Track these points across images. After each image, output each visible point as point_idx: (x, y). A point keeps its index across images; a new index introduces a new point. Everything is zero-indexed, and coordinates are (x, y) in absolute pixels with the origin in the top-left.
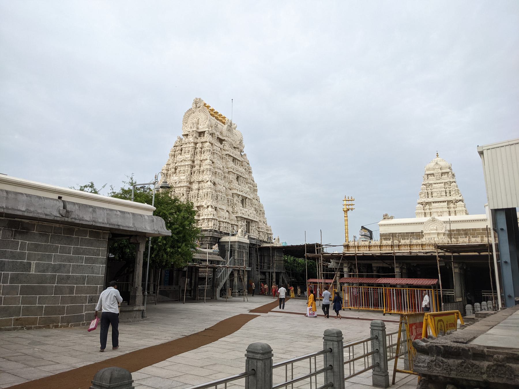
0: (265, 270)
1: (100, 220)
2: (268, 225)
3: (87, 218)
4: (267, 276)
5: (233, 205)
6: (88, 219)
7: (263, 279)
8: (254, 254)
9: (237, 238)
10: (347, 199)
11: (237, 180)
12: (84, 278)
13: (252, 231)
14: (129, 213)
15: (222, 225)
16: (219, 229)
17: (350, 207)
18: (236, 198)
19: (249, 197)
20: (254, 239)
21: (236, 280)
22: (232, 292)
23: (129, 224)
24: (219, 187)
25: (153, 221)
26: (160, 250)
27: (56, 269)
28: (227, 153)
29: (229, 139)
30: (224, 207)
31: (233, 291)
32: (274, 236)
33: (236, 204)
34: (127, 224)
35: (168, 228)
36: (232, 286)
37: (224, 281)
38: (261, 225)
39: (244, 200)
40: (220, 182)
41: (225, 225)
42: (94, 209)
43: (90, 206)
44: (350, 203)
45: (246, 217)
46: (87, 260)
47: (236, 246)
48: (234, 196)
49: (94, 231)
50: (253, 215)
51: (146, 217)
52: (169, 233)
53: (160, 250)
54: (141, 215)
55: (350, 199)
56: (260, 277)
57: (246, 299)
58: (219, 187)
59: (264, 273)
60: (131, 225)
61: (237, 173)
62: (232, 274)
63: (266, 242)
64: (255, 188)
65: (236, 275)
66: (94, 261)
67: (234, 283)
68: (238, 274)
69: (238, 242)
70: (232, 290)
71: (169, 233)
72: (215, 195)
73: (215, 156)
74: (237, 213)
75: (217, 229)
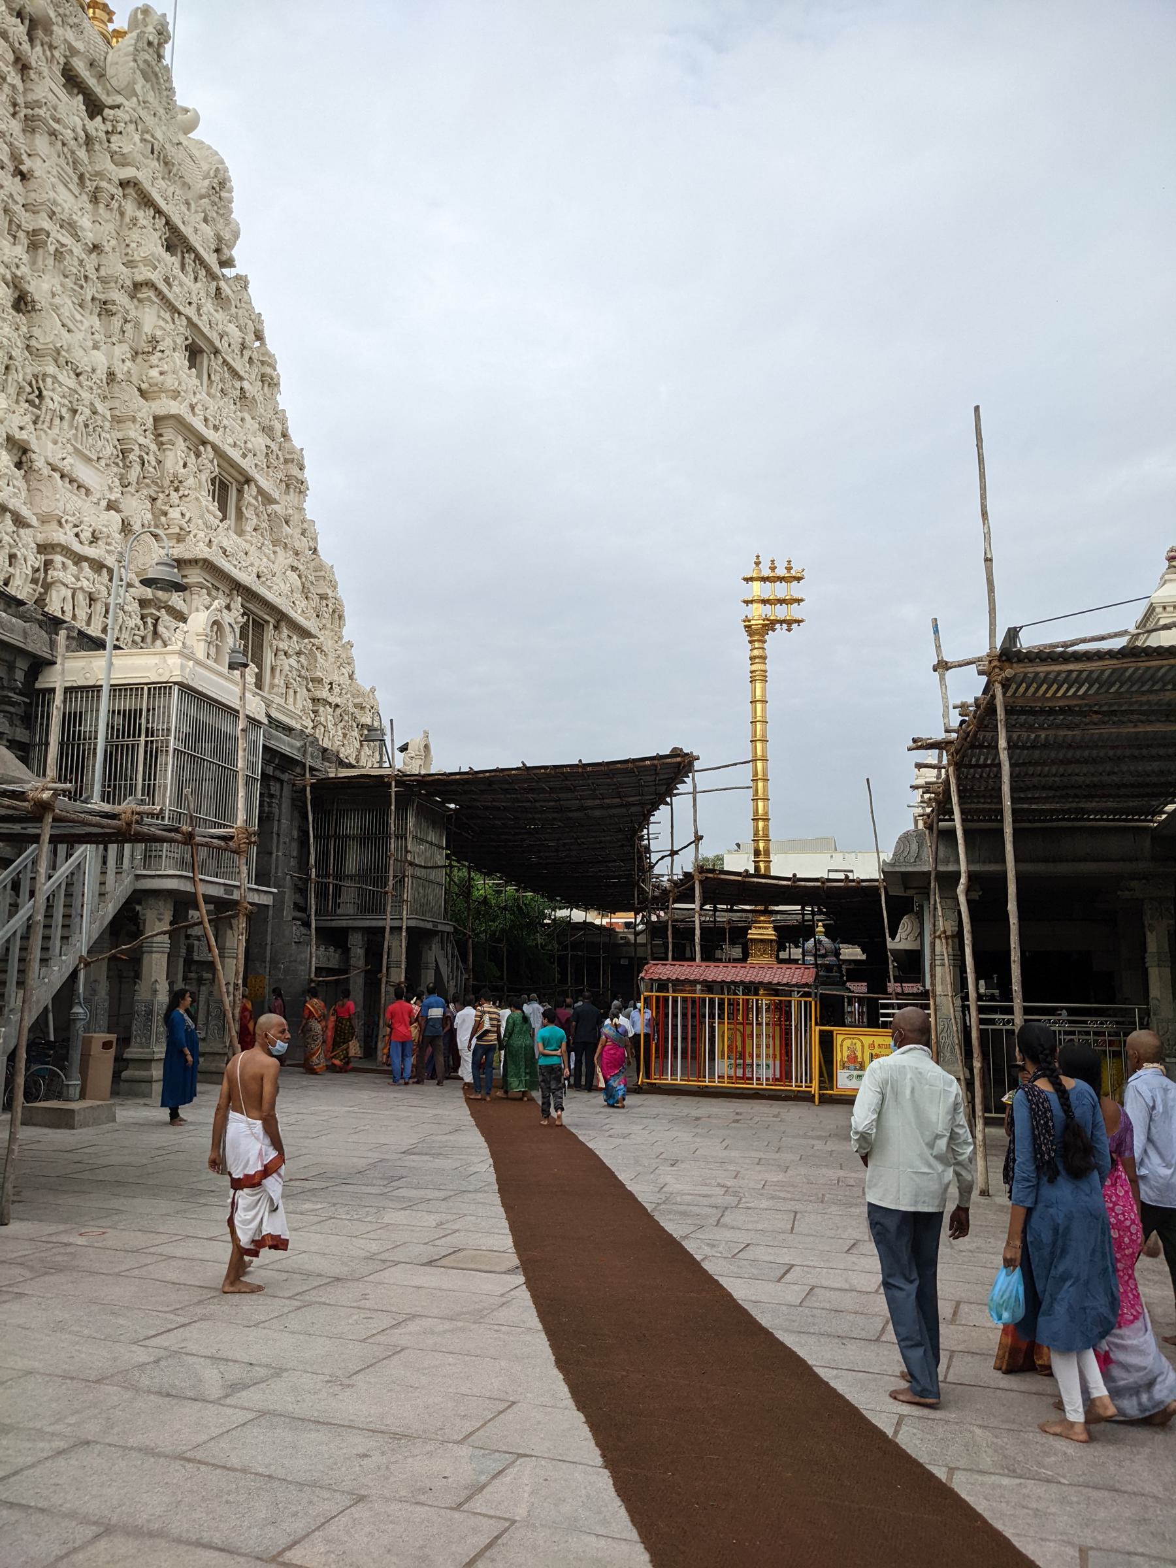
0: (347, 915)
2: (364, 680)
4: (358, 953)
5: (161, 490)
7: (330, 971)
8: (285, 823)
9: (174, 661)
10: (766, 572)
11: (192, 363)
13: (279, 680)
15: (64, 573)
16: (40, 602)
17: (781, 612)
18: (176, 455)
19: (257, 476)
20: (288, 730)
21: (157, 968)
22: (121, 1063)
24: (49, 332)
28: (128, 173)
29: (150, 121)
30: (84, 473)
31: (133, 1052)
32: (393, 742)
33: (177, 484)
36: (123, 1023)
37: (57, 974)
38: (325, 667)
39: (228, 486)
40: (67, 305)
41: (87, 579)
44: (781, 590)
45: (246, 578)
47: (173, 717)
48: (169, 434)
50: (285, 588)
55: (781, 571)
56: (314, 956)
57: (246, 1140)
58: (49, 332)
59: (334, 937)
61: (190, 312)
62: (126, 924)
63: (354, 767)
64: (295, 471)
65: (157, 924)
67: (143, 992)
68: (180, 932)
69: (187, 690)
70: (125, 1041)
72: (26, 369)
73: (41, 142)
74: (180, 539)
75: (21, 589)
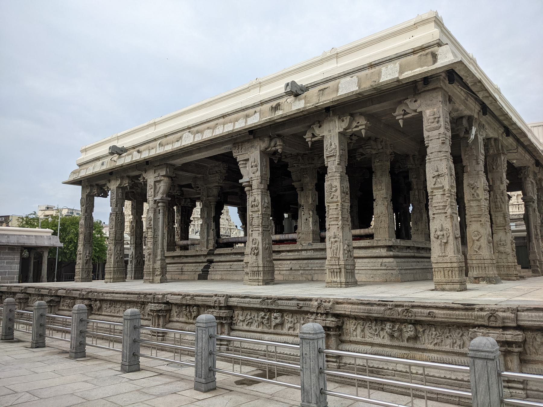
1: (13, 242)
6: (4, 242)
12: (6, 272)
14: (32, 236)
23: (32, 242)
25: (50, 239)
26: (71, 254)
34: (31, 242)
35: (61, 242)
42: (8, 236)
43: (6, 235)
46: (7, 263)
49: (12, 248)
51: (45, 237)
52: (62, 245)
53: (71, 254)
54: (41, 236)
60: (34, 242)
66: (12, 263)
71: (62, 245)
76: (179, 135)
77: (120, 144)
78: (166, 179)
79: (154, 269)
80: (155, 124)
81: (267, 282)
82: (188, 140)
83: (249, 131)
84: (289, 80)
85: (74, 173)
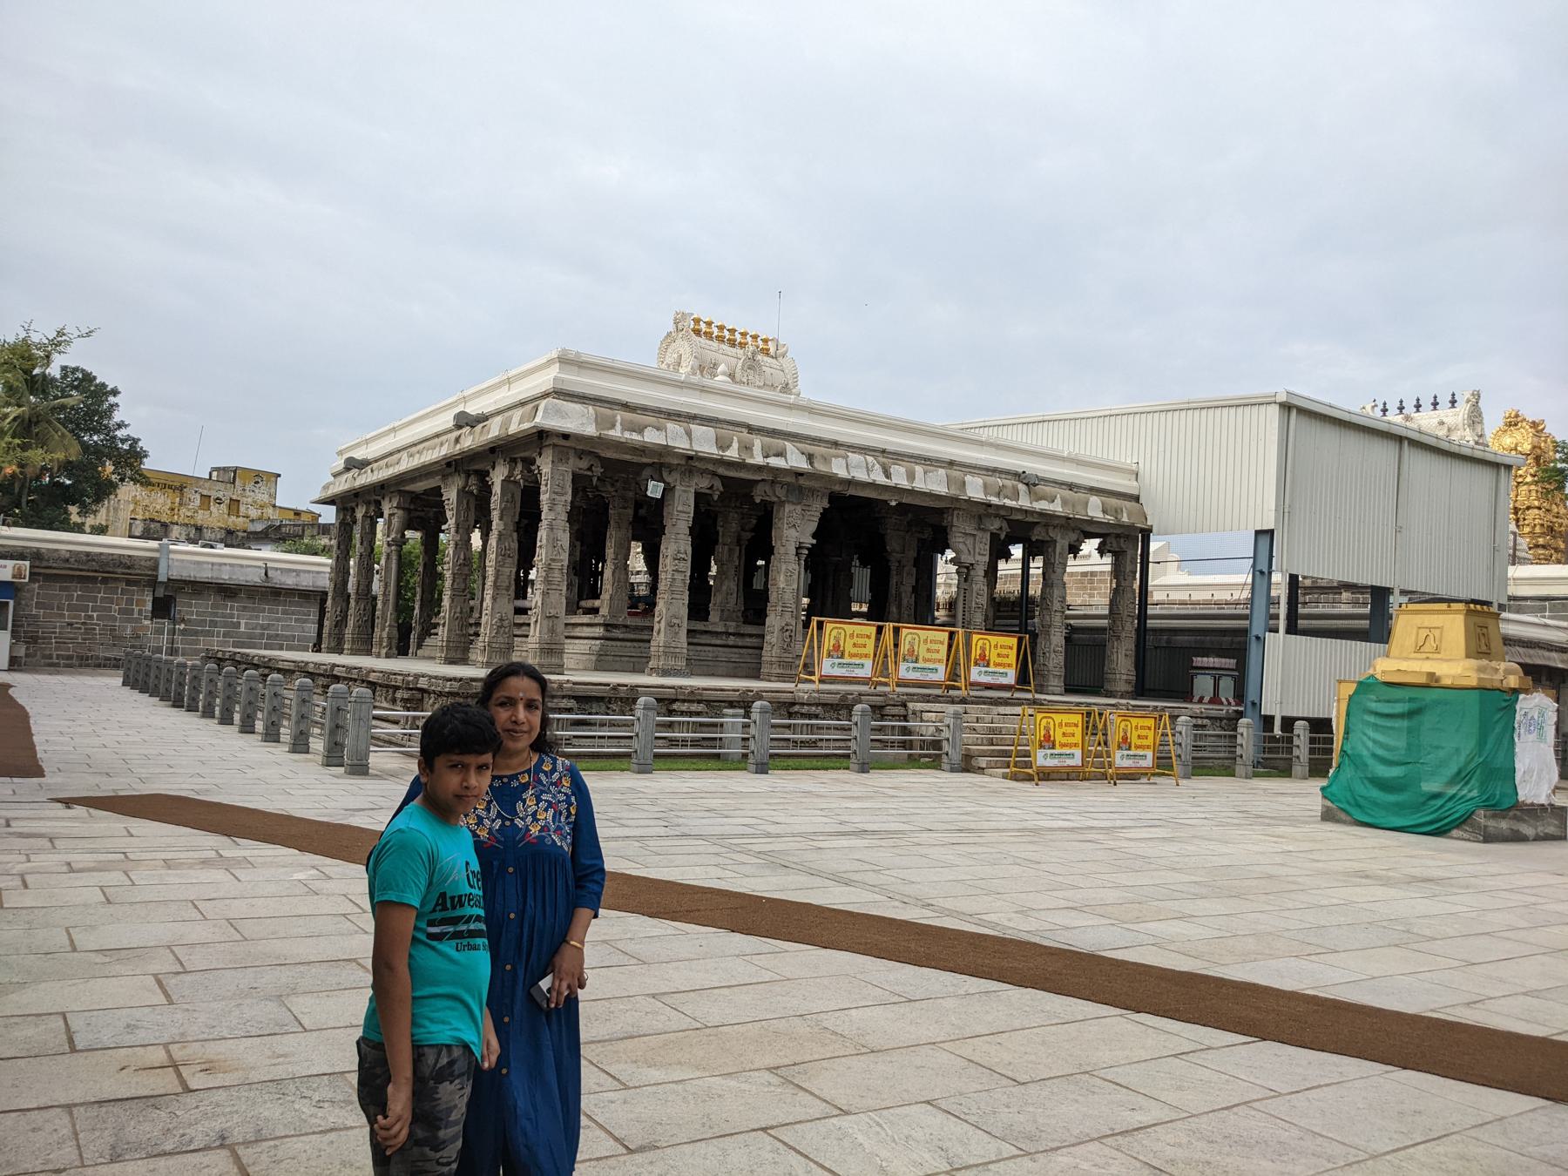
3: (290, 581)
27: (263, 627)
42: (298, 572)
66: (305, 621)
76: (396, 456)
77: (359, 454)
78: (400, 512)
79: (381, 638)
80: (394, 430)
81: (450, 661)
82: (406, 464)
83: (449, 464)
84: (457, 410)
85: (326, 487)
